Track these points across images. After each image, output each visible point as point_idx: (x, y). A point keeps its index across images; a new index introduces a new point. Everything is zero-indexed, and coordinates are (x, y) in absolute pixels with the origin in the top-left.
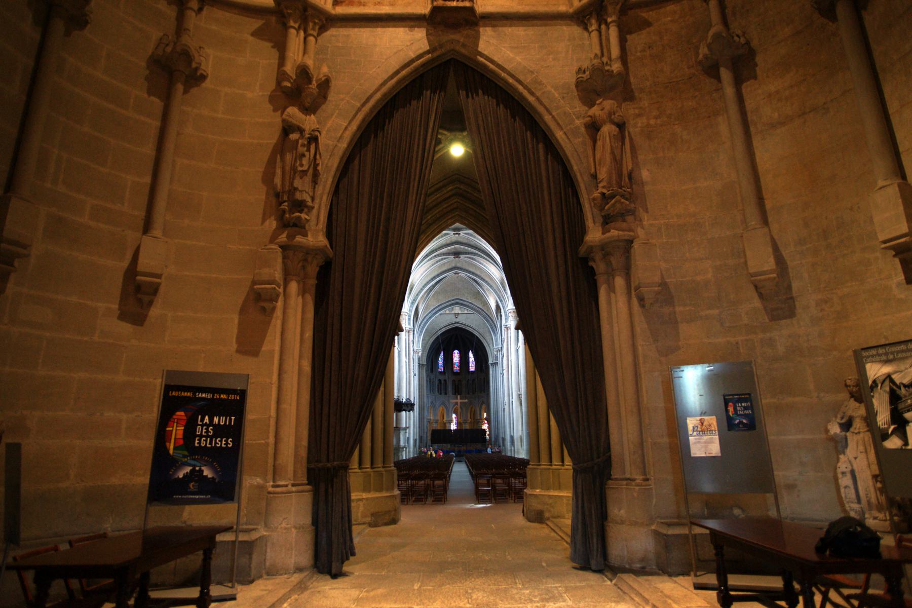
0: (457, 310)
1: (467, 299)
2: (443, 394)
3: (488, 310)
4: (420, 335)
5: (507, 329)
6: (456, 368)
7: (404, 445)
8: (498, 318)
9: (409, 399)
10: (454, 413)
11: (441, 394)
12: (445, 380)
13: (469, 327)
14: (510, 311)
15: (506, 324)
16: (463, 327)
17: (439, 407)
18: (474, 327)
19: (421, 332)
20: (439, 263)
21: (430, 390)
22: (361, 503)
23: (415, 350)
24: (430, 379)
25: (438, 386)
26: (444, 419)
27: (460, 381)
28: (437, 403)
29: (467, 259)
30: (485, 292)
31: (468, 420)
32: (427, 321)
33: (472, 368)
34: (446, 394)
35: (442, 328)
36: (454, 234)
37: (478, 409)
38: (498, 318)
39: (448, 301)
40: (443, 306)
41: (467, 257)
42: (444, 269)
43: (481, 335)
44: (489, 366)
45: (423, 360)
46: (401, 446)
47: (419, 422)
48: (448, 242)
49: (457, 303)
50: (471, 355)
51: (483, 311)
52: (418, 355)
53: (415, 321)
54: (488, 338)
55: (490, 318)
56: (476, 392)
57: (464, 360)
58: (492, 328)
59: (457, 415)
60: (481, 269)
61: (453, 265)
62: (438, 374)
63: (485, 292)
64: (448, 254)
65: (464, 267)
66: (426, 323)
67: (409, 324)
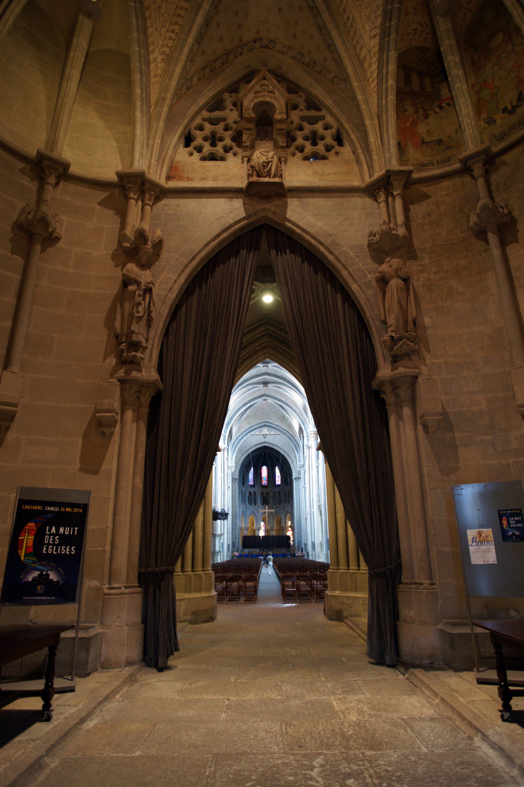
0: (265, 431)
1: (274, 422)
2: (253, 504)
3: (292, 432)
4: (233, 453)
5: (309, 448)
6: (265, 482)
7: (219, 549)
8: (300, 438)
9: (223, 509)
10: (263, 521)
11: (251, 504)
12: (255, 493)
14: (311, 433)
15: (308, 444)
17: (249, 516)
18: (280, 446)
19: (234, 450)
20: (250, 391)
21: (242, 501)
22: (183, 603)
23: (229, 466)
24: (242, 491)
25: (249, 497)
26: (253, 526)
27: (267, 493)
28: (248, 513)
29: (274, 388)
30: (289, 416)
33: (278, 481)
34: (255, 504)
36: (263, 366)
37: (283, 518)
38: (300, 438)
39: (258, 424)
40: (253, 428)
41: (275, 386)
42: (254, 396)
43: (286, 452)
46: (217, 551)
47: (232, 529)
48: (258, 373)
49: (265, 426)
51: (288, 432)
54: (292, 456)
55: (294, 438)
56: (281, 502)
57: (271, 475)
58: (295, 447)
59: (265, 523)
60: (286, 396)
61: (263, 393)
62: (248, 486)
63: (289, 416)
64: (259, 383)
65: (272, 395)
66: (238, 443)
67: (224, 443)
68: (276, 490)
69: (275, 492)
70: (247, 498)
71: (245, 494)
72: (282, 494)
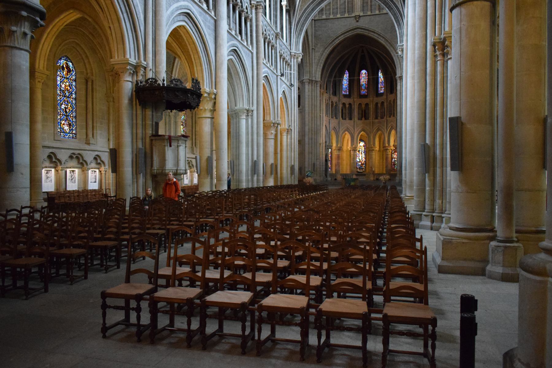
2: (347, 119)
4: (300, 34)
7: (175, 169)
11: (345, 119)
13: (374, 32)
16: (366, 33)
19: (301, 30)
24: (332, 102)
25: (342, 110)
27: (367, 105)
31: (376, 148)
32: (308, 14)
35: (340, 36)
43: (387, 41)
44: (396, 81)
45: (317, 76)
50: (380, 75)
52: (297, 61)
53: (292, 15)
57: (373, 81)
62: (342, 97)
68: (380, 100)
69: (377, 104)
70: (340, 111)
71: (336, 106)
72: (385, 104)
